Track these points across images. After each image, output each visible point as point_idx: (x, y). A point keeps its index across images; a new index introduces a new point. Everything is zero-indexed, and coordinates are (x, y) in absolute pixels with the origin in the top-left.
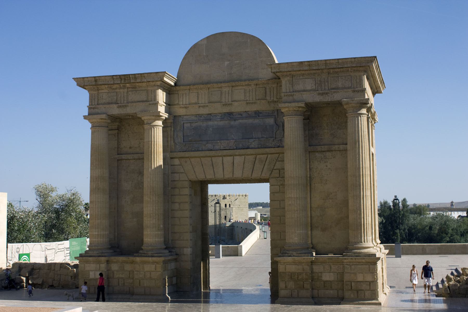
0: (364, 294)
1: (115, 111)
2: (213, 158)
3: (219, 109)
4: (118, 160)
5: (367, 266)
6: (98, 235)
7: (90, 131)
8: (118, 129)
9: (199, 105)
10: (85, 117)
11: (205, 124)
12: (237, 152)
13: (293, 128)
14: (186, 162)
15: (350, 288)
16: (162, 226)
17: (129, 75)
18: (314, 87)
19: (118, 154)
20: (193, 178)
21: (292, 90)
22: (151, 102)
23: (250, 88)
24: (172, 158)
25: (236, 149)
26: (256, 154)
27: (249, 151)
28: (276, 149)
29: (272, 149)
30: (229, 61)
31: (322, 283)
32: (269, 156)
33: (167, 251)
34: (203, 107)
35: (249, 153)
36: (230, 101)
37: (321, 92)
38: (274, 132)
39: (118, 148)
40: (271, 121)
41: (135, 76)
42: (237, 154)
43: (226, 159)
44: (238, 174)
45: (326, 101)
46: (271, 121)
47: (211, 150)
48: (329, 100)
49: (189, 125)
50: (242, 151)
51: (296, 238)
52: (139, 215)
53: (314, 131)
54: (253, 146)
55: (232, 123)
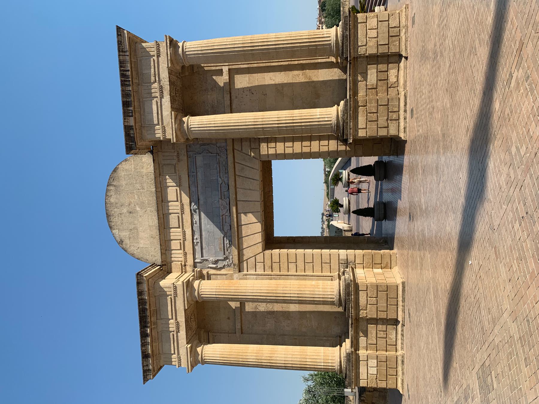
4: (242, 333)
12: (232, 196)
17: (140, 317)
20: (260, 247)
27: (231, 183)
28: (228, 151)
29: (229, 156)
31: (380, 83)
32: (236, 161)
34: (184, 233)
35: (233, 183)
38: (210, 155)
39: (229, 333)
42: (234, 196)
47: (230, 226)
50: (232, 190)
53: (209, 110)
54: (226, 179)
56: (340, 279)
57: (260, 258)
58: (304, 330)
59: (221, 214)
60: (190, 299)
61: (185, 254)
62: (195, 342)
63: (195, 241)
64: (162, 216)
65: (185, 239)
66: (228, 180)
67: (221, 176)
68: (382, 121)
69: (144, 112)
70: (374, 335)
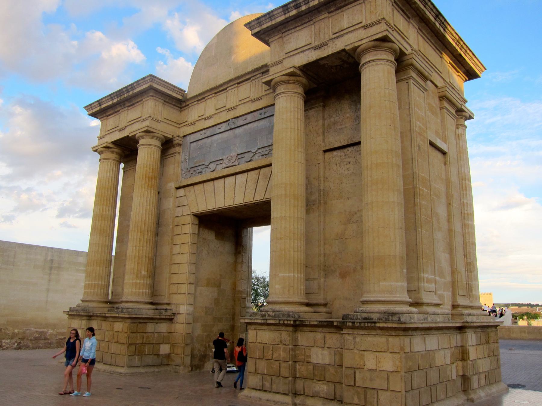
6: (89, 284)
14: (190, 191)
15: (352, 384)
26: (260, 168)
31: (311, 367)
34: (209, 118)
42: (238, 171)
45: (326, 55)
49: (195, 144)
51: (277, 286)
55: (237, 131)
59: (224, 157)
61: (193, 124)
64: (224, 87)
65: (206, 119)
67: (259, 151)
68: (263, 366)
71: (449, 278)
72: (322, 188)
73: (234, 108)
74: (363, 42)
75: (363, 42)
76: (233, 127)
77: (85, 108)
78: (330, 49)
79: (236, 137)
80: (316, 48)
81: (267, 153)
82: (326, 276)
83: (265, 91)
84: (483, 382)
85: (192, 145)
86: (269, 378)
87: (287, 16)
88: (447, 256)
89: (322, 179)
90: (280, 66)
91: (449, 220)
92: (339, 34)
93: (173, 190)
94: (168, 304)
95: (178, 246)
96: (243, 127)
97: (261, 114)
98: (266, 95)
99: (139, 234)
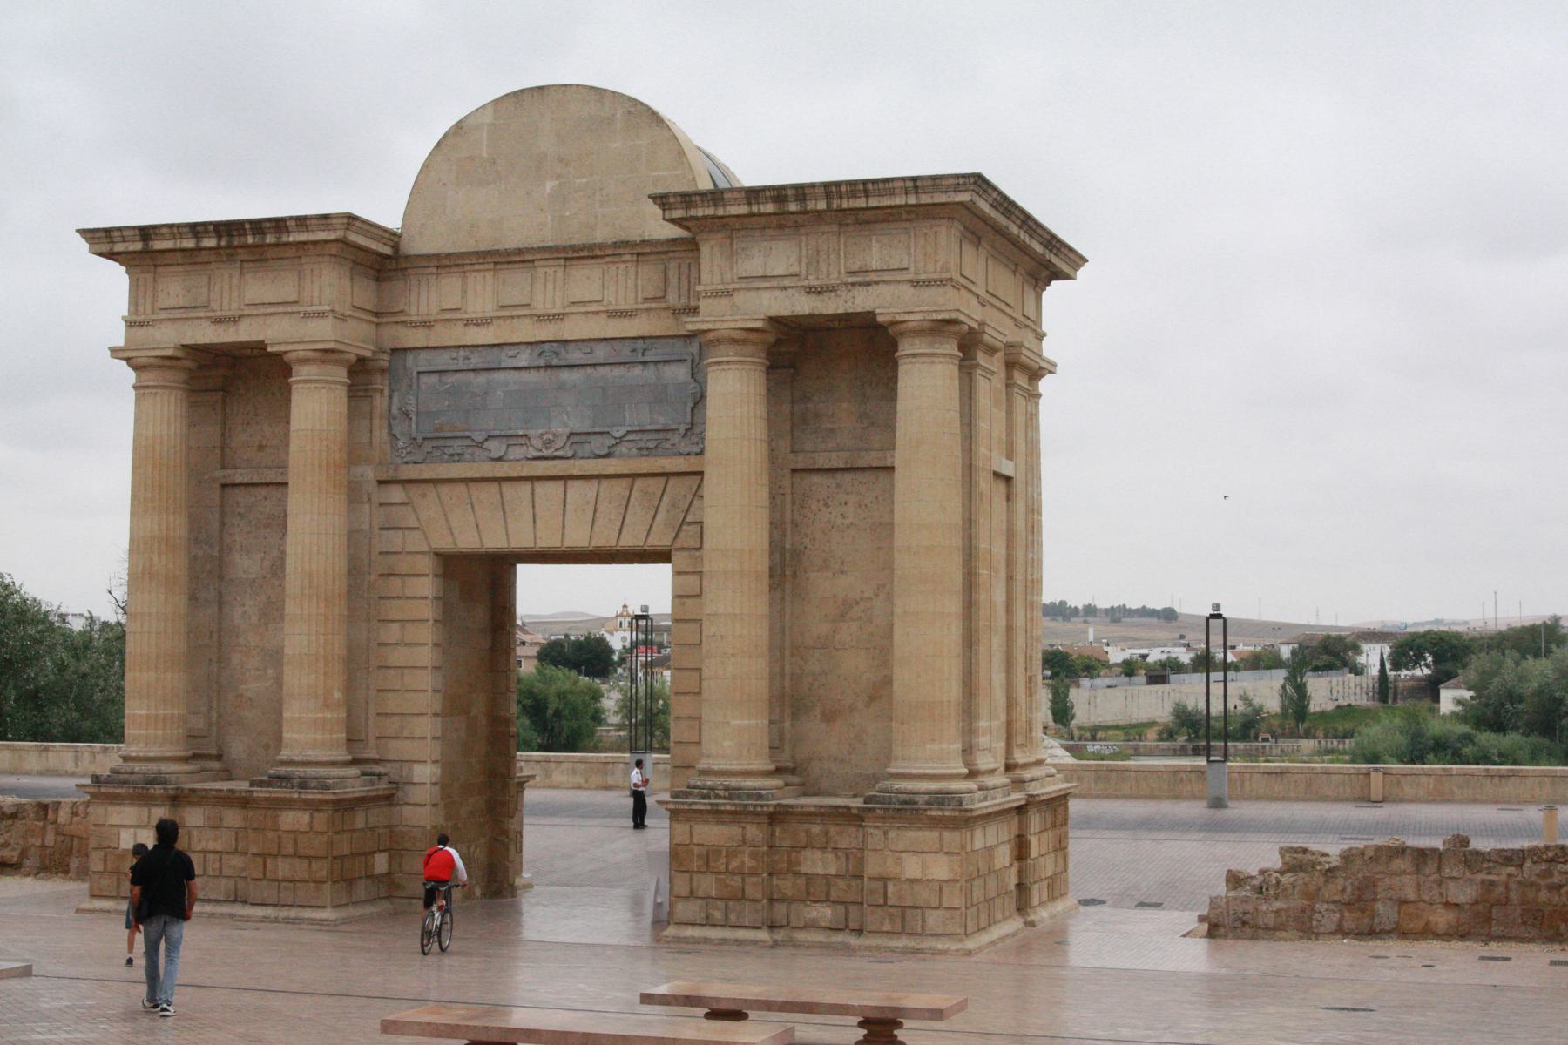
0: (923, 921)
1: (206, 334)
2: (506, 487)
3: (527, 331)
4: (224, 486)
5: (935, 834)
6: (148, 716)
7: (132, 394)
8: (223, 390)
9: (466, 316)
10: (115, 352)
11: (482, 379)
13: (735, 397)
14: (424, 496)
15: (881, 902)
16: (337, 695)
18: (794, 269)
19: (223, 468)
20: (444, 544)
21: (728, 277)
22: (309, 309)
23: (622, 266)
24: (380, 482)
25: (573, 457)
26: (634, 476)
29: (681, 460)
30: (559, 176)
31: (801, 881)
33: (353, 771)
35: (611, 471)
36: (558, 305)
37: (816, 283)
38: (690, 405)
40: (680, 373)
41: (258, 226)
42: (575, 472)
43: (541, 488)
44: (578, 538)
45: (831, 311)
46: (680, 373)
47: (500, 459)
48: (841, 311)
49: (434, 379)
51: (726, 743)
52: (275, 657)
55: (565, 375)
56: (355, 762)
57: (415, 541)
58: (236, 659)
59: (531, 432)
60: (292, 356)
61: (427, 324)
62: (189, 364)
63: (462, 352)
65: (468, 323)
66: (621, 456)
69: (772, 238)
70: (211, 846)
71: (1003, 717)
72: (788, 546)
73: (558, 317)
74: (912, 317)
75: (912, 317)
76: (555, 362)
77: (84, 233)
78: (841, 302)
79: (562, 387)
80: (810, 291)
81: (651, 445)
82: (795, 716)
83: (646, 299)
84: (1045, 897)
85: (424, 379)
86: (721, 904)
87: (755, 209)
88: (1003, 676)
89: (788, 527)
90: (724, 301)
91: (1009, 610)
92: (862, 279)
93: (371, 486)
94: (377, 762)
95: (395, 626)
96: (582, 371)
97: (634, 351)
98: (648, 310)
99: (322, 605)
